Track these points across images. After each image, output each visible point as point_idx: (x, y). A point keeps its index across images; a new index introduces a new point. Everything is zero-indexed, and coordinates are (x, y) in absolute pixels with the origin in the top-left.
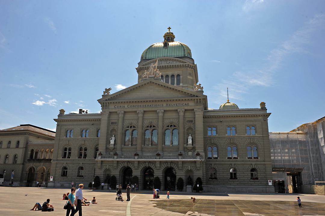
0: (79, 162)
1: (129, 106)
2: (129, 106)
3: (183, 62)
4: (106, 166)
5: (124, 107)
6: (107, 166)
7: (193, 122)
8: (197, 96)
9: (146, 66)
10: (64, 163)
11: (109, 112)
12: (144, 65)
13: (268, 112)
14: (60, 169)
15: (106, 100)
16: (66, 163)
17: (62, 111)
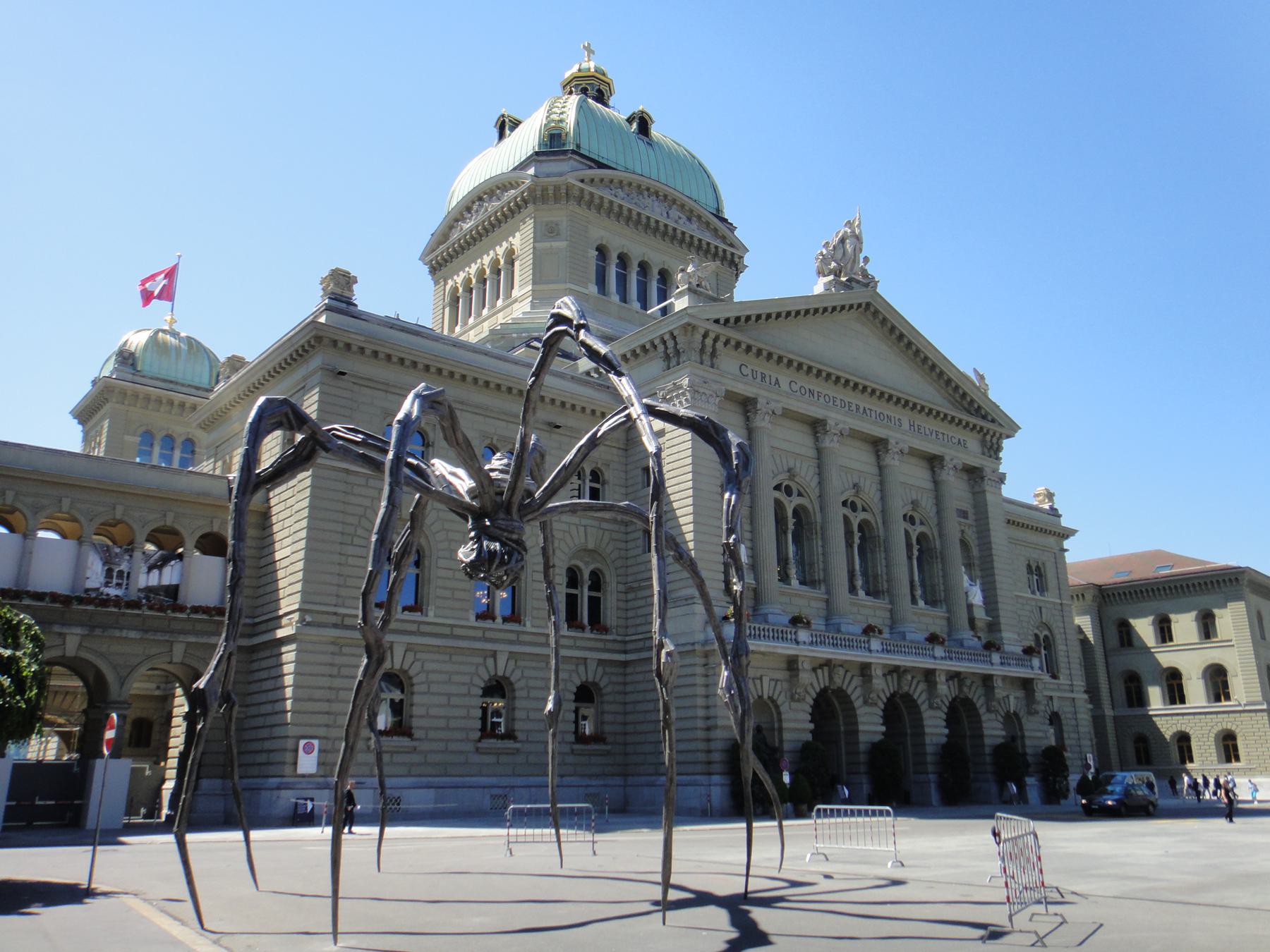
0: (489, 646)
1: (795, 387)
2: (795, 387)
3: (724, 239)
4: (758, 682)
5: (777, 382)
6: (761, 679)
7: (966, 518)
8: (993, 421)
9: (598, 192)
10: (494, 655)
11: (727, 391)
12: (582, 181)
13: (1065, 522)
14: (469, 694)
15: (717, 321)
16: (409, 648)
17: (340, 291)
